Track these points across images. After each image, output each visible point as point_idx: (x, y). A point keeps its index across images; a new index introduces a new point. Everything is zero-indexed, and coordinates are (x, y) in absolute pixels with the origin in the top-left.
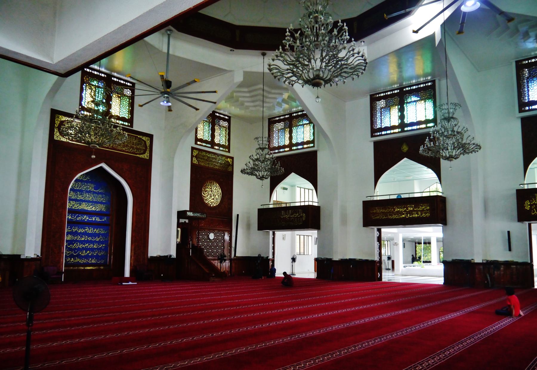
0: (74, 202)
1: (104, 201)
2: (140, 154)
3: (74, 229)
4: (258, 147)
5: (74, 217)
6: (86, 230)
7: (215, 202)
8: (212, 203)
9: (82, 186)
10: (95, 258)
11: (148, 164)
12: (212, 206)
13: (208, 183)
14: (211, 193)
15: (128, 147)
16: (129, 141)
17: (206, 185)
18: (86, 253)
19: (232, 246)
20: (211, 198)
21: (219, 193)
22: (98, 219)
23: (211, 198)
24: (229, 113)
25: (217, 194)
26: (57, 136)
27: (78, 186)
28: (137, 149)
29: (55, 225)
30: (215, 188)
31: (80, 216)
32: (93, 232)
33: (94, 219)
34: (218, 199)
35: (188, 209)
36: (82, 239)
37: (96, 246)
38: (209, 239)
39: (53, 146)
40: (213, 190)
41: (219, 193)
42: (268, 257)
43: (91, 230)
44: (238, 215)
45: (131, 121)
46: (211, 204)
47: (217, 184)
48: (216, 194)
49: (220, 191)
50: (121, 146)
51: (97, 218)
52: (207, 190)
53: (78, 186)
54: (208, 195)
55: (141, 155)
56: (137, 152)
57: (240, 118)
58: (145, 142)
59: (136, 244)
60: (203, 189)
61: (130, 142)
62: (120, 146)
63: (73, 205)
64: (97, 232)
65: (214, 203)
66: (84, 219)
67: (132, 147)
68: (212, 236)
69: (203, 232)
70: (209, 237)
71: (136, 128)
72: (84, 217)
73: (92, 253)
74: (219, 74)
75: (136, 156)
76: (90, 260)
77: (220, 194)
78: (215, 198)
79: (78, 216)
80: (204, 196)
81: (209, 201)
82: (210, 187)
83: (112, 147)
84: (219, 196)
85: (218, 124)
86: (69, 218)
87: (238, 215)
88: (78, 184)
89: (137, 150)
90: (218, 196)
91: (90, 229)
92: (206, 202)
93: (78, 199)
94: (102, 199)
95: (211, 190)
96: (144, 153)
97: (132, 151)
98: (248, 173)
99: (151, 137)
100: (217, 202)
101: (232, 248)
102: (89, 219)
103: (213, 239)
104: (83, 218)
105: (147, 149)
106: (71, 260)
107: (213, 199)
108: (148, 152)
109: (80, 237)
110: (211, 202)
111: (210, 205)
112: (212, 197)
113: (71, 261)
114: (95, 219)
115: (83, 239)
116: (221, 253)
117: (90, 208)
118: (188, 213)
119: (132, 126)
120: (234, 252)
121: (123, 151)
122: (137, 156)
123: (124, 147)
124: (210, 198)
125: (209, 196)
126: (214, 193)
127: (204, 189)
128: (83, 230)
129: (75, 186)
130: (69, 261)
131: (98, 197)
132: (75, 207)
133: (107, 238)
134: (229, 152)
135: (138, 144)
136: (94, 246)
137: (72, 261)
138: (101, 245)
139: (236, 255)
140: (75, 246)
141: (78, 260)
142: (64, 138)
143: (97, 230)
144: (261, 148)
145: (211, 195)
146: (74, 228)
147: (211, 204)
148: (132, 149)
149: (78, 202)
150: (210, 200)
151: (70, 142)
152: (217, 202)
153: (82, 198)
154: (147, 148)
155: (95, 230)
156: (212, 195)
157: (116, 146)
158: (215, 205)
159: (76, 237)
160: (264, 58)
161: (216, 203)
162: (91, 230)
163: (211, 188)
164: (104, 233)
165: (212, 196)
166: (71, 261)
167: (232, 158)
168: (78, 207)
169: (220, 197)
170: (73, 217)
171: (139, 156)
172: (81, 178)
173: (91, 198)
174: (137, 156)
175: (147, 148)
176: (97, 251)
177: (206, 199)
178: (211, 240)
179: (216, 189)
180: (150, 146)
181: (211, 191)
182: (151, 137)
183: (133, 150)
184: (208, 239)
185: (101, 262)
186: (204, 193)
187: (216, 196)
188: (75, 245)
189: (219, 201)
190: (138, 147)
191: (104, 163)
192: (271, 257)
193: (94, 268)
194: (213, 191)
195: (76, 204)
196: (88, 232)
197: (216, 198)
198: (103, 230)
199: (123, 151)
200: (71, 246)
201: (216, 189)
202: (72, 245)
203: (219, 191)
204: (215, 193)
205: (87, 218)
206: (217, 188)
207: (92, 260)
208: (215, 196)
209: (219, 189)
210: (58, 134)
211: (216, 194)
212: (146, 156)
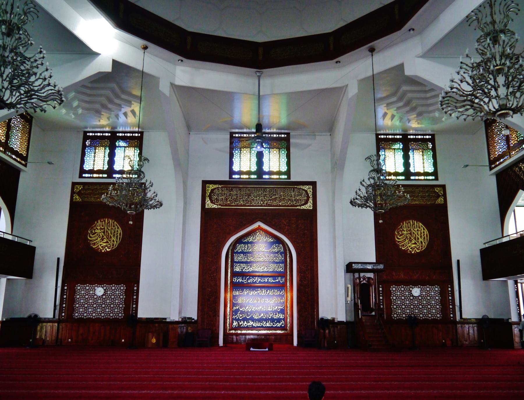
0: (245, 264)
1: (277, 261)
2: (300, 206)
3: (245, 292)
4: (372, 169)
5: (245, 279)
6: (259, 292)
7: (417, 247)
8: (414, 248)
9: (252, 247)
10: (270, 322)
11: (312, 215)
12: (413, 253)
13: (403, 224)
14: (410, 235)
15: (285, 201)
16: (286, 194)
17: (401, 227)
18: (260, 315)
19: (456, 305)
20: (411, 243)
21: (424, 235)
22: (271, 280)
23: (411, 243)
24: (415, 131)
25: (421, 237)
26: (209, 204)
27: (248, 248)
28: (297, 200)
29: (210, 290)
30: (416, 230)
31: (251, 279)
32: (266, 293)
33: (266, 281)
34: (423, 243)
35: (374, 261)
36: (255, 302)
37: (271, 308)
38: (413, 296)
39: (205, 213)
40: (414, 231)
41: (424, 235)
42: (508, 320)
43: (264, 292)
44: (458, 261)
45: (288, 173)
46: (411, 250)
47: (420, 224)
48: (419, 237)
49: (425, 232)
50: (277, 201)
51: (269, 279)
52: (403, 233)
53: (248, 248)
54: (405, 239)
55: (302, 207)
56: (297, 204)
57: (443, 132)
58: (306, 191)
59: (302, 305)
60: (396, 233)
61: (287, 195)
62: (275, 201)
63: (244, 268)
64: (270, 293)
65: (417, 248)
66: (256, 281)
67: (290, 200)
68: (416, 291)
69: (402, 287)
70: (412, 293)
71: (293, 179)
72: (255, 279)
73: (267, 316)
74: (342, 94)
75: (296, 208)
76: (264, 324)
77: (425, 235)
78: (418, 242)
79: (249, 279)
80: (399, 242)
81: (407, 247)
82: (409, 229)
83: (267, 204)
84: (424, 238)
85: (428, 148)
86: (240, 280)
87: (458, 261)
88: (248, 246)
89: (296, 202)
90: (423, 238)
91: (262, 291)
92: (403, 249)
93: (248, 261)
94: (275, 258)
95: (409, 232)
96: (306, 203)
97: (290, 204)
98: (359, 206)
99: (313, 184)
100: (422, 246)
101: (456, 307)
102: (261, 281)
103: (419, 296)
104: (255, 280)
105: (310, 199)
106: (244, 323)
107: (415, 243)
108: (311, 200)
109: (252, 299)
110: (411, 248)
111: (410, 251)
112: (413, 242)
113: (244, 324)
114: (268, 280)
115: (256, 302)
116: (412, 314)
117: (261, 269)
118: (353, 265)
119: (289, 177)
120: (459, 313)
121: (280, 206)
122: (298, 208)
123: (281, 201)
124: (409, 243)
125: (407, 241)
126: (415, 235)
127: (398, 232)
128: (256, 292)
129: (244, 249)
130: (242, 325)
131: (270, 257)
132: (245, 270)
133: (283, 299)
134: (437, 179)
135: (297, 195)
136: (268, 309)
137: (246, 325)
138: (277, 307)
139: (464, 317)
140: (247, 309)
141: (251, 323)
142: (215, 204)
143: (270, 291)
144: (374, 170)
145: (410, 238)
146: (245, 291)
147: (411, 250)
148: (290, 202)
149: (249, 265)
150: (410, 245)
151: (222, 207)
152: (422, 246)
153: (252, 260)
154: (310, 197)
155: (269, 292)
156: (412, 238)
157: (271, 202)
158: (418, 251)
159: (248, 300)
160: (372, 55)
161: (420, 248)
162: (264, 292)
163: (410, 230)
164: (278, 294)
165: (412, 240)
166: (244, 324)
167: (443, 187)
168: (248, 269)
169: (427, 239)
170: (244, 280)
171: (299, 208)
172: (250, 240)
173: (262, 259)
174: (298, 208)
175: (310, 197)
176: (271, 314)
177: (403, 245)
178: (416, 297)
179: (418, 230)
180: (313, 194)
181: (411, 234)
182: (313, 184)
183: (291, 203)
184: (411, 296)
185: (277, 325)
186: (399, 237)
187: (420, 239)
188: (247, 308)
189: (425, 245)
190: (298, 198)
191: (259, 222)
192: (514, 318)
193: (282, 332)
194: (414, 233)
195: (246, 267)
196: (260, 294)
197: (420, 242)
198: (278, 291)
199: (280, 206)
200: (243, 309)
201: (418, 230)
202: (244, 308)
203: (424, 232)
204: (417, 235)
205: (259, 280)
206: (420, 228)
207: (266, 322)
208: (418, 239)
209: (424, 229)
210: (209, 202)
211: (419, 237)
212: (309, 206)
